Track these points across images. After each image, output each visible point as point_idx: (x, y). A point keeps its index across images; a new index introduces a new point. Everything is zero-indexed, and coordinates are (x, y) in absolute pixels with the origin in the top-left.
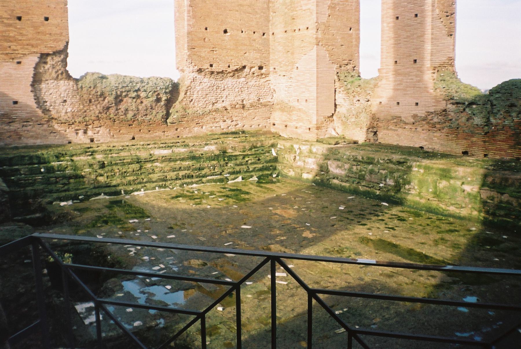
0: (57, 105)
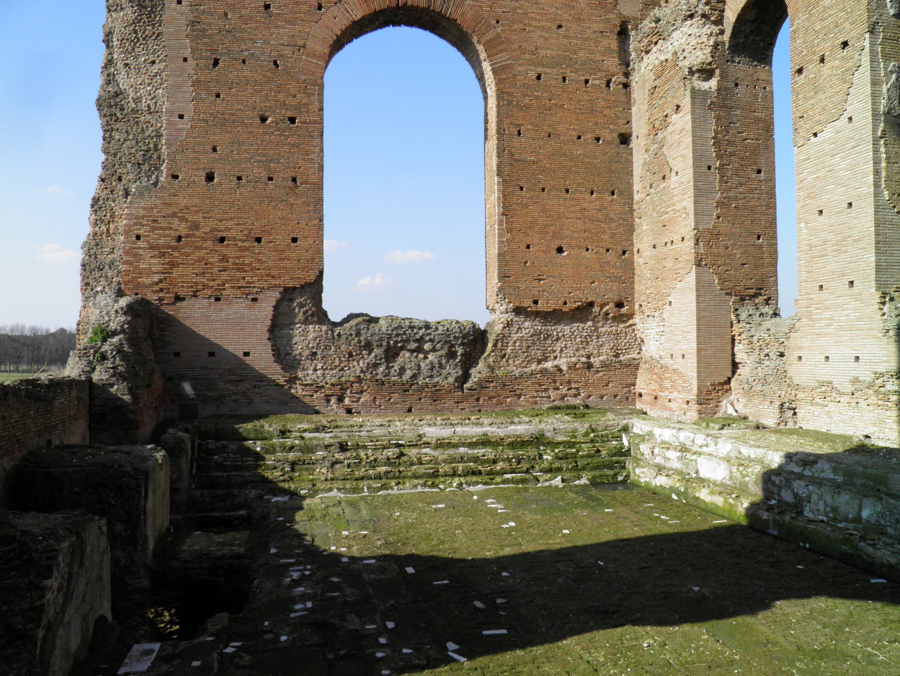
0: (303, 358)
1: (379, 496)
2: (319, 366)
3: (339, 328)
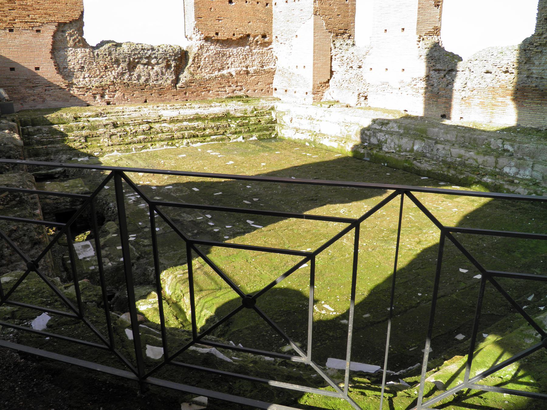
0: (76, 71)
1: (143, 153)
2: (87, 75)
3: (97, 50)
